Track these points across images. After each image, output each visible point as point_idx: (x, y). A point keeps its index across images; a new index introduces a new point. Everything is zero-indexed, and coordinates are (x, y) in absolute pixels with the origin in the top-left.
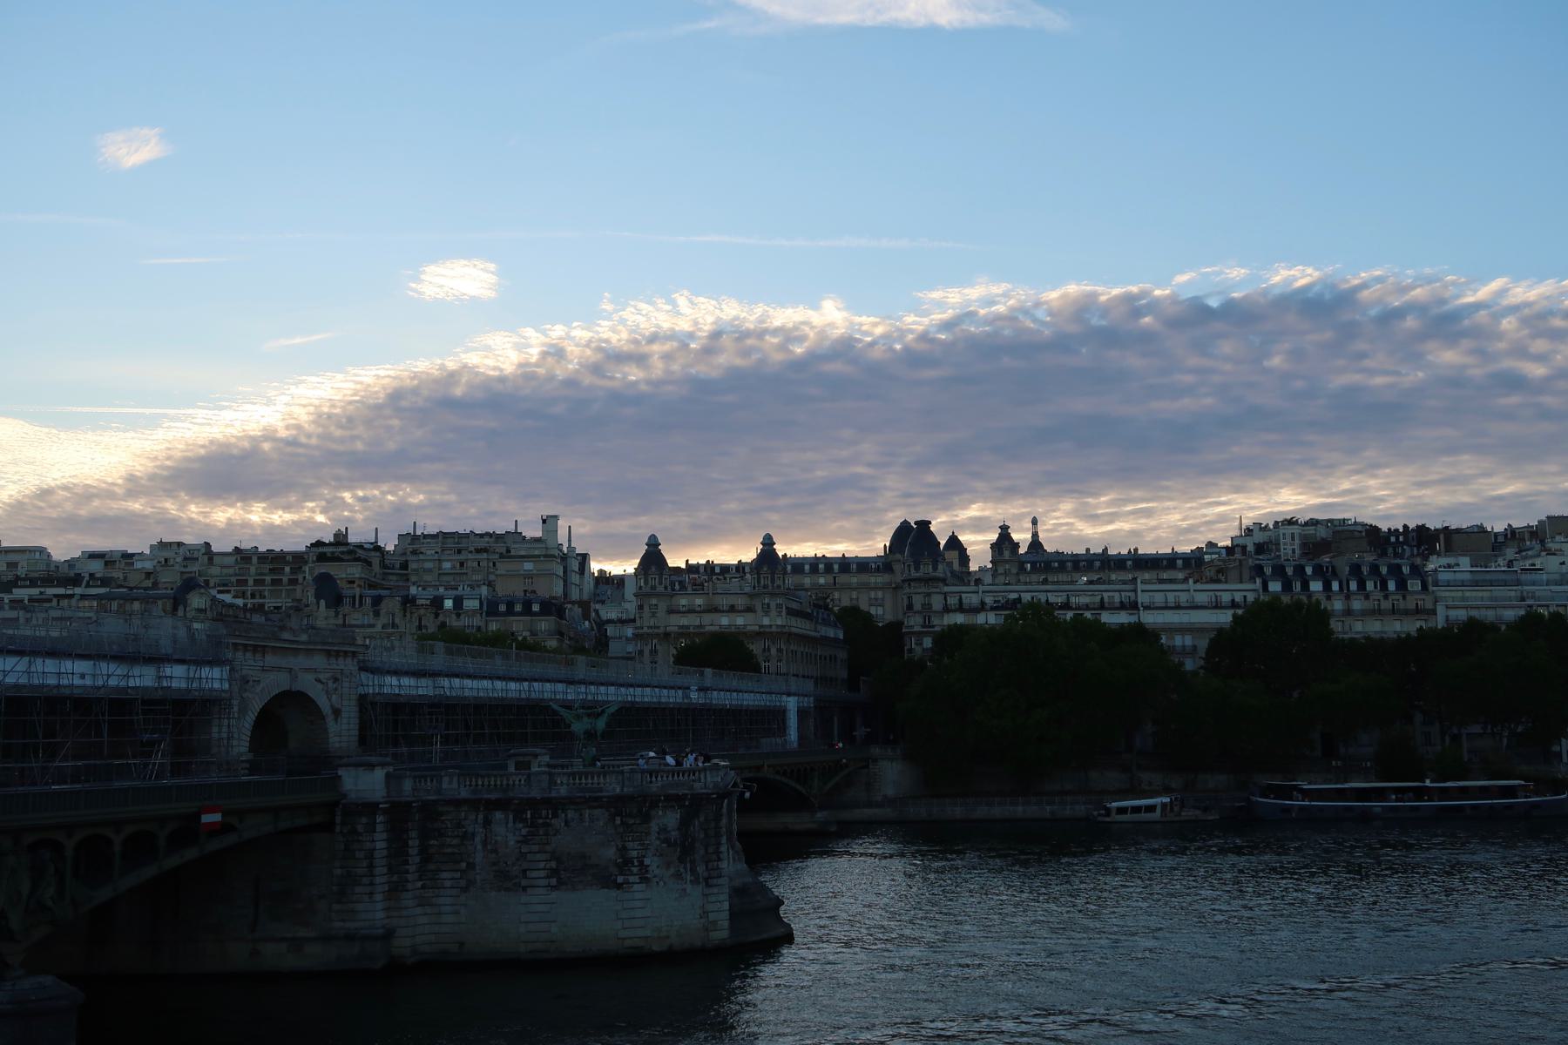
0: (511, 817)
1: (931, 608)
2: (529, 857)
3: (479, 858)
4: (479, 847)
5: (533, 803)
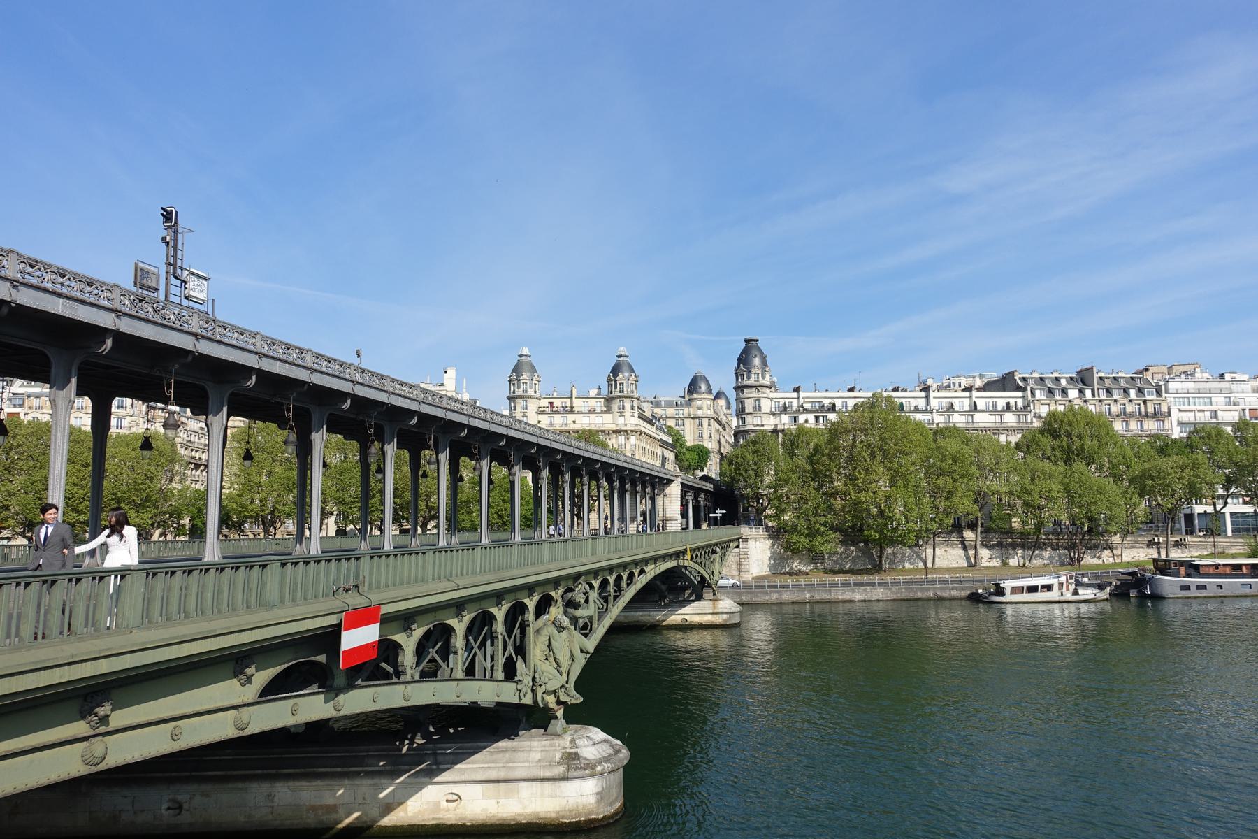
1: (760, 410)
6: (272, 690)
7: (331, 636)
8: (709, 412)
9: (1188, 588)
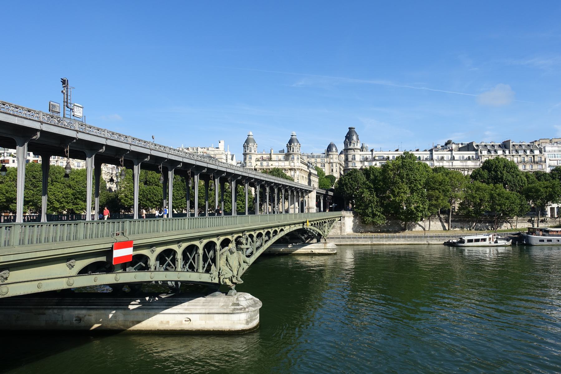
6: (84, 271)
7: (109, 253)
8: (336, 160)
9: (543, 241)
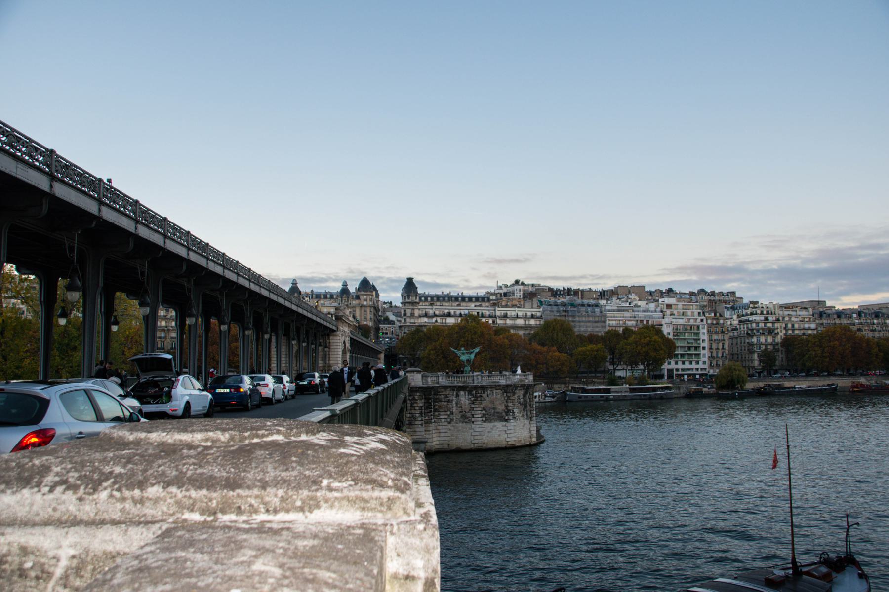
0: (467, 393)
2: (475, 409)
3: (454, 410)
4: (455, 405)
5: (476, 388)
